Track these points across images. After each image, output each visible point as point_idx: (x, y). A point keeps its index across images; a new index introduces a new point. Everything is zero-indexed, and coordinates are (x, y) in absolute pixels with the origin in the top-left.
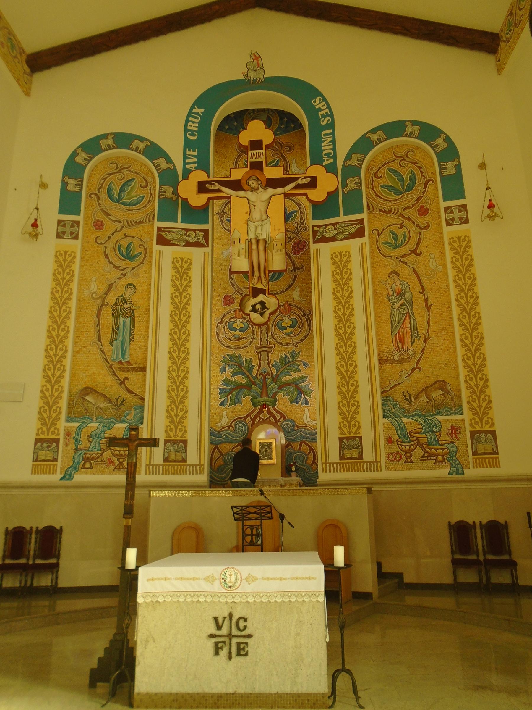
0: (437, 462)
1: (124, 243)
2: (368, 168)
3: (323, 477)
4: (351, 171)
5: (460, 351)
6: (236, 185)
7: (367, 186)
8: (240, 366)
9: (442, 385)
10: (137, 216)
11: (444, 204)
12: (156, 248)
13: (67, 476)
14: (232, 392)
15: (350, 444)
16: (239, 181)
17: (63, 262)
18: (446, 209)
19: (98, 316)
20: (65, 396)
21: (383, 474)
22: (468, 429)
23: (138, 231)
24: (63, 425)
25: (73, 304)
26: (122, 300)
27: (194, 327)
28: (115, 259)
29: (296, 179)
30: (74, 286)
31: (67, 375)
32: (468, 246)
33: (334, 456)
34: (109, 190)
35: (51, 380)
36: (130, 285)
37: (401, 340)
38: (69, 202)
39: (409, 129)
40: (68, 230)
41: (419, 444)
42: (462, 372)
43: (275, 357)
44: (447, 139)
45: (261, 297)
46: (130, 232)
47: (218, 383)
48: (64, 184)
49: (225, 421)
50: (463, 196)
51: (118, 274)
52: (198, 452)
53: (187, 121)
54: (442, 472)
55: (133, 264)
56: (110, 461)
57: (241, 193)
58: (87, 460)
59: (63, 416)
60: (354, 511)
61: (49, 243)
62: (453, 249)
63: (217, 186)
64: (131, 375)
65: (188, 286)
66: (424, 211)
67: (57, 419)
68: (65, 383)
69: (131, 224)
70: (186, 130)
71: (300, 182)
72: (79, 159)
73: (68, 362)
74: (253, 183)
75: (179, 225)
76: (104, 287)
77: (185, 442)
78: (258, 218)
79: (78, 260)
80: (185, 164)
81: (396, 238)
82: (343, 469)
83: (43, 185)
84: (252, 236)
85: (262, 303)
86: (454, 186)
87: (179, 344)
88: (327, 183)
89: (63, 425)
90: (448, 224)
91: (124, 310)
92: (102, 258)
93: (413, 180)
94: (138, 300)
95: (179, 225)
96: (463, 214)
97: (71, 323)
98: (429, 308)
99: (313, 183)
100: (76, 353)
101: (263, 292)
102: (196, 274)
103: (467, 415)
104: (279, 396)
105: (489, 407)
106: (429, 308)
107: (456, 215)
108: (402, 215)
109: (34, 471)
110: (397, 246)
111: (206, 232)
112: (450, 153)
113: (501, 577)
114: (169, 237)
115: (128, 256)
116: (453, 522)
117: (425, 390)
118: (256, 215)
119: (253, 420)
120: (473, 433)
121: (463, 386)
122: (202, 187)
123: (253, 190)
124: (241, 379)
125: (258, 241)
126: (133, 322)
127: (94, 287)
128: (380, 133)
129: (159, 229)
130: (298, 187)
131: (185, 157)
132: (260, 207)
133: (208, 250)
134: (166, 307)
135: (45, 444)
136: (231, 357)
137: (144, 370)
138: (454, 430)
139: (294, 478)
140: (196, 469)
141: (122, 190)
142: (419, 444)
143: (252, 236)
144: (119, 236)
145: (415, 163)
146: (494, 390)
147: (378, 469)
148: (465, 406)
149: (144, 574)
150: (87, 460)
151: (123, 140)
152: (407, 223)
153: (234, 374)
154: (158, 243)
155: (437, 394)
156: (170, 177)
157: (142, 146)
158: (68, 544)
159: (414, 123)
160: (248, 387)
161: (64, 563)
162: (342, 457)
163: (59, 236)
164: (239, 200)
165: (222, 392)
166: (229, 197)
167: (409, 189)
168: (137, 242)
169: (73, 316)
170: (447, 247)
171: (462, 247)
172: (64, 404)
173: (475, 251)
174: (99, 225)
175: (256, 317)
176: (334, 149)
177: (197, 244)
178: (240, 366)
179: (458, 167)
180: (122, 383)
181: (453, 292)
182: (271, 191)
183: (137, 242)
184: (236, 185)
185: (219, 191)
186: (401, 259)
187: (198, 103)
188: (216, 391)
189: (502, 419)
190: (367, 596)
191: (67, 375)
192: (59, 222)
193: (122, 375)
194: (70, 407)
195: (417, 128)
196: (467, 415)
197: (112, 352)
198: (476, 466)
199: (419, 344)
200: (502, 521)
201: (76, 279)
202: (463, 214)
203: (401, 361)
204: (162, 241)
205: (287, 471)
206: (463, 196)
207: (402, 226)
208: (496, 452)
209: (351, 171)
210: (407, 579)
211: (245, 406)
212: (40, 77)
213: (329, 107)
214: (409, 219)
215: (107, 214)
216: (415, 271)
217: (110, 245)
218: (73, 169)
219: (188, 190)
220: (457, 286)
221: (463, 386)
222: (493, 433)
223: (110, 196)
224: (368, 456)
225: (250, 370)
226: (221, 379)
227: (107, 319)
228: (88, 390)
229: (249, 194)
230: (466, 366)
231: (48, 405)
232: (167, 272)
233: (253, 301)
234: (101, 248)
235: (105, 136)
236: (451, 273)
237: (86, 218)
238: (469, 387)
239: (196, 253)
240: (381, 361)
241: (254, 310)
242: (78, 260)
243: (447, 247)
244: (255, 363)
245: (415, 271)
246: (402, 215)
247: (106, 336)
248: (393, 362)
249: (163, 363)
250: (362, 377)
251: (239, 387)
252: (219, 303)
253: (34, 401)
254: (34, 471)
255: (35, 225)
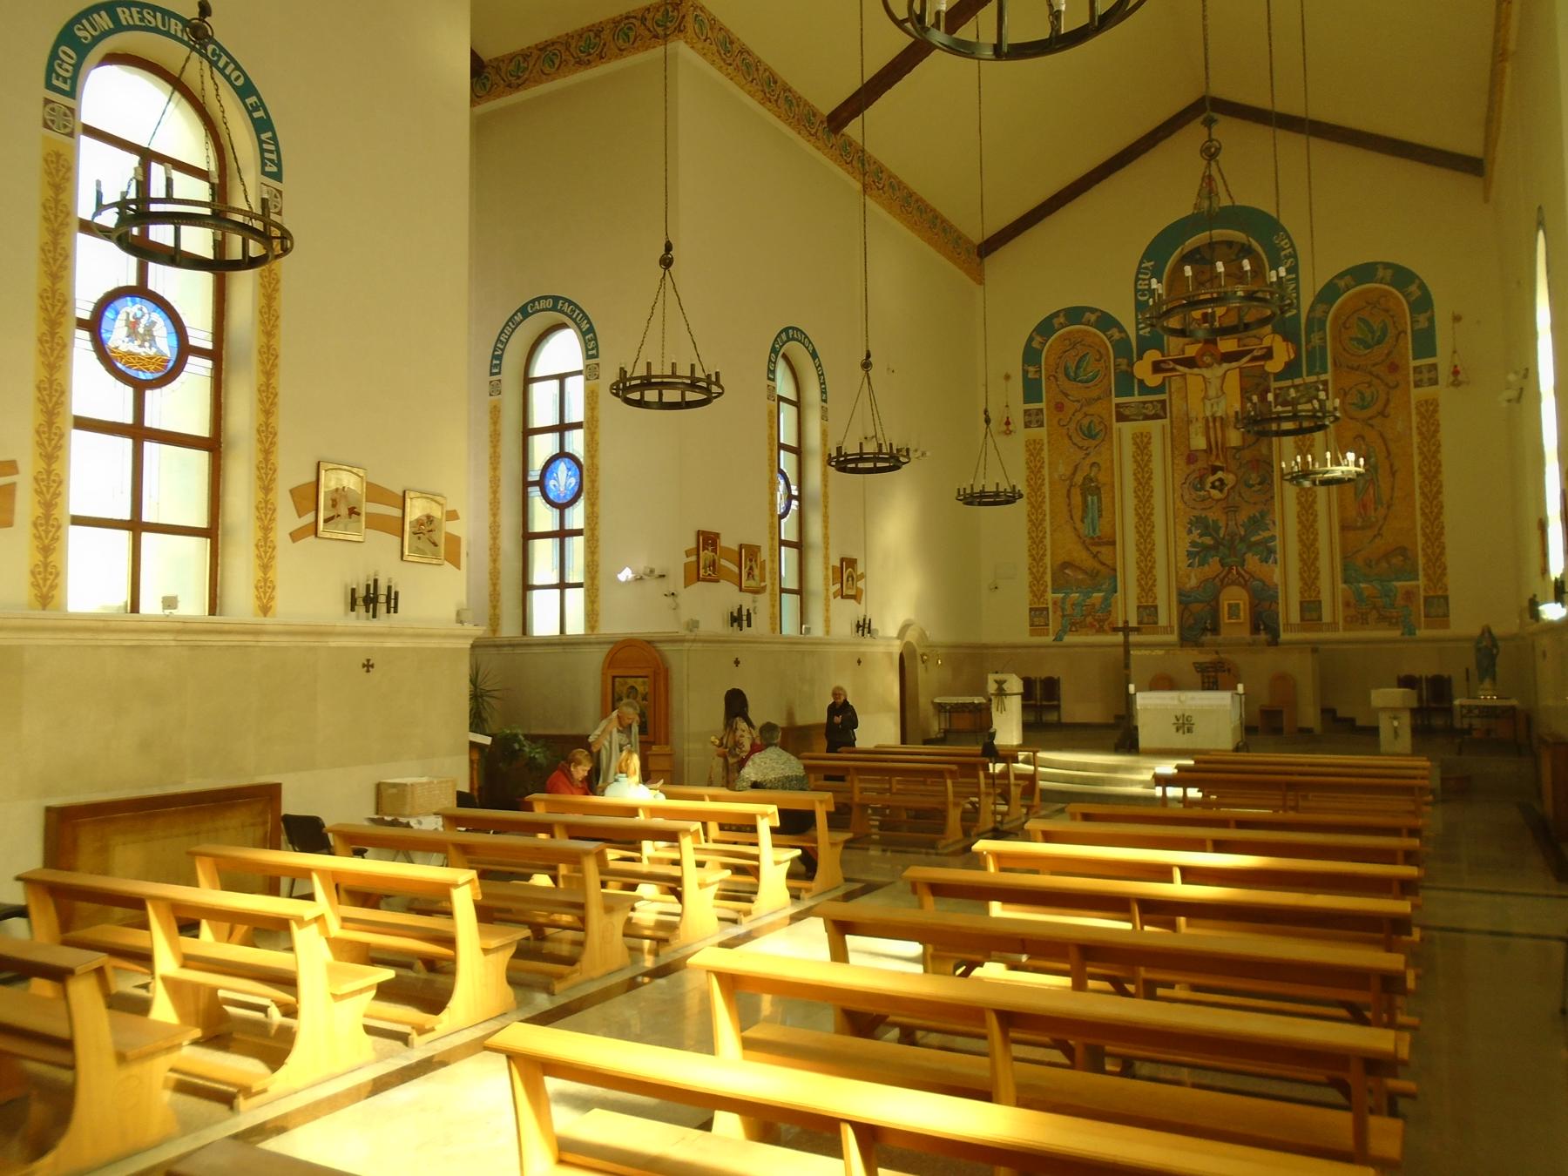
0: (1390, 624)
1: (1086, 422)
2: (1336, 318)
3: (1284, 636)
4: (1316, 324)
5: (1419, 519)
6: (1190, 363)
7: (1334, 338)
8: (1207, 527)
9: (1402, 551)
10: (1095, 393)
11: (1413, 363)
12: (1116, 425)
13: (1058, 638)
14: (1199, 554)
15: (1310, 608)
16: (1192, 359)
17: (1033, 449)
18: (1415, 368)
19: (1068, 497)
20: (1049, 571)
21: (1341, 634)
22: (1422, 593)
23: (1095, 409)
24: (1050, 596)
25: (1046, 489)
26: (1088, 479)
27: (1158, 501)
28: (1076, 439)
29: (1251, 351)
30: (1046, 471)
31: (1048, 553)
32: (1435, 411)
33: (1295, 617)
34: (1066, 368)
35: (1036, 559)
36: (1094, 464)
37: (1364, 506)
38: (1032, 391)
39: (1381, 273)
40: (1033, 418)
41: (1375, 607)
42: (1420, 540)
43: (1243, 517)
44: (1423, 287)
45: (1220, 474)
46: (1091, 410)
47: (1184, 545)
48: (1025, 372)
49: (1193, 582)
50: (1434, 355)
51: (1082, 454)
52: (1167, 613)
53: (1137, 279)
54: (1396, 633)
55: (1094, 443)
56: (1092, 626)
57: (1196, 370)
58: (1073, 624)
59: (1049, 589)
60: (1301, 668)
61: (1021, 434)
62: (1419, 413)
63: (1172, 365)
64: (1104, 549)
65: (1149, 461)
66: (1394, 368)
67: (1045, 591)
68: (1048, 560)
69: (1089, 402)
70: (1137, 291)
71: (1256, 353)
72: (1035, 344)
73: (1048, 542)
74: (1207, 359)
75: (1137, 398)
76: (1071, 469)
77: (1156, 607)
78: (1214, 394)
79: (1046, 447)
80: (1138, 330)
81: (1363, 399)
82: (1305, 630)
83: (1007, 377)
84: (1208, 414)
85: (1220, 480)
86: (1425, 343)
87: (1144, 520)
88: (1282, 353)
89: (1050, 596)
90: (1417, 385)
91: (1091, 488)
92: (1066, 440)
93: (1384, 332)
94: (1102, 478)
95: (1137, 398)
96: (1432, 375)
97: (1047, 507)
98: (1393, 474)
99: (1268, 354)
100: (1053, 531)
101: (1221, 469)
102: (1156, 448)
103: (1422, 581)
104: (1249, 556)
105: (1444, 574)
106: (1393, 474)
107: (1425, 376)
108: (1371, 373)
109: (1033, 633)
110: (1363, 408)
111: (1163, 402)
112: (1423, 303)
113: (1438, 722)
114: (1127, 412)
115: (1092, 437)
116: (1403, 674)
117: (1386, 556)
118: (1212, 392)
119: (1222, 581)
120: (1426, 599)
121: (1420, 552)
122: (1157, 367)
123: (1208, 366)
124: (1208, 540)
125: (1214, 419)
126: (1100, 499)
127: (1062, 469)
128: (1348, 278)
129: (1117, 405)
130: (1255, 359)
131: (1138, 323)
132: (1217, 383)
133: (1166, 422)
134: (1130, 484)
135: (1038, 615)
136: (1197, 518)
137: (1113, 543)
138: (1409, 595)
139: (1263, 636)
140: (1167, 630)
141: (1078, 367)
142: (1375, 607)
143: (1208, 414)
144: (1079, 416)
145: (1387, 311)
146: (1450, 558)
147: (1336, 629)
148: (1421, 573)
149: (1139, 696)
150: (1073, 624)
151: (1074, 314)
152: (1375, 381)
153: (1201, 536)
154: (1118, 420)
155: (1397, 560)
156: (1122, 347)
157: (1093, 318)
158: (1065, 690)
159: (1387, 266)
160: (1215, 547)
161: (1064, 705)
162: (1302, 619)
163: (1027, 425)
164: (1194, 377)
165: (1190, 554)
166: (1183, 376)
167: (1379, 343)
168: (1096, 420)
169: (1047, 500)
170: (1414, 412)
171: (1429, 411)
172: (1048, 578)
173: (1443, 417)
174: (1059, 407)
175: (1215, 493)
176: (1298, 298)
177: (1156, 417)
178: (1207, 527)
179: (1431, 320)
180: (1095, 556)
181: (1417, 459)
182: (1225, 366)
183: (1096, 420)
184: (1190, 363)
185: (1173, 370)
186: (1367, 422)
187: (1147, 256)
188: (1182, 554)
189: (1457, 583)
190: (1309, 731)
191: (1048, 553)
192: (1026, 411)
193: (1095, 549)
194: (1054, 580)
195: (1389, 272)
196: (1422, 581)
197: (1085, 529)
198: (1427, 626)
199: (1382, 511)
200: (1446, 674)
201: (1046, 465)
202: (1432, 375)
203: (1363, 528)
204: (1121, 418)
205: (1255, 629)
206: (1434, 355)
207: (1370, 385)
208: (1446, 615)
209: (1316, 324)
210: (1359, 723)
211: (1213, 566)
212: (987, 260)
213: (1292, 246)
214: (1378, 377)
215: (1066, 395)
216: (1381, 435)
217: (1072, 426)
218: (1031, 356)
219: (1143, 370)
220: (1421, 453)
221: (1420, 552)
222: (1446, 598)
223: (1067, 375)
224: (1327, 617)
225: (1217, 530)
226: (1188, 539)
227: (1077, 499)
228: (1066, 565)
229: (1204, 371)
230: (1425, 534)
231: (1036, 579)
232: (1129, 449)
233: (1211, 479)
234: (1064, 431)
235: (1056, 315)
236: (1416, 439)
237: (1048, 402)
238: (1425, 555)
239: (1154, 426)
240: (1344, 528)
241: (1213, 487)
242: (1046, 447)
243: (1414, 412)
244: (1222, 524)
245: (1381, 435)
246: (1371, 373)
247: (1078, 514)
248: (1356, 528)
249: (1131, 537)
250: (1323, 544)
251: (1206, 549)
252: (1181, 461)
253: (1024, 578)
254: (1033, 633)
255: (1008, 423)
